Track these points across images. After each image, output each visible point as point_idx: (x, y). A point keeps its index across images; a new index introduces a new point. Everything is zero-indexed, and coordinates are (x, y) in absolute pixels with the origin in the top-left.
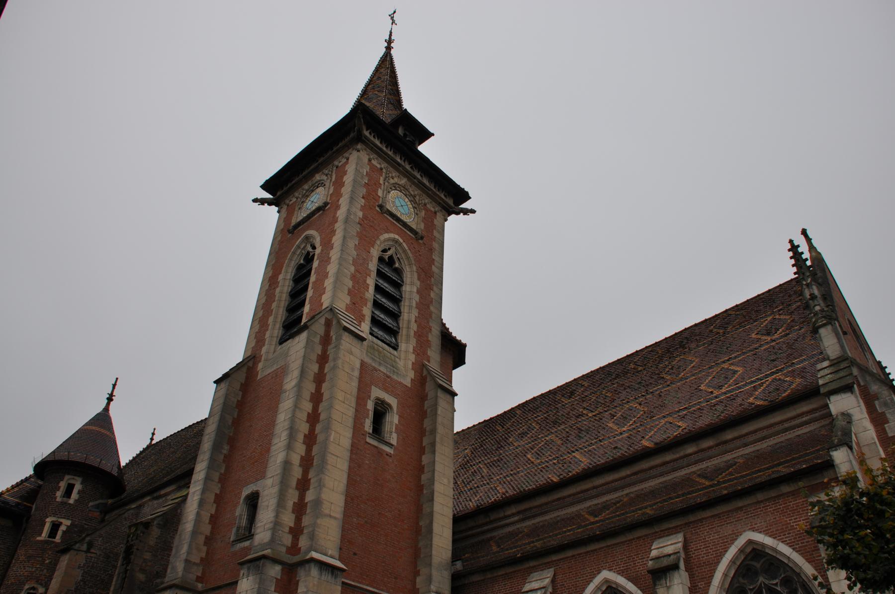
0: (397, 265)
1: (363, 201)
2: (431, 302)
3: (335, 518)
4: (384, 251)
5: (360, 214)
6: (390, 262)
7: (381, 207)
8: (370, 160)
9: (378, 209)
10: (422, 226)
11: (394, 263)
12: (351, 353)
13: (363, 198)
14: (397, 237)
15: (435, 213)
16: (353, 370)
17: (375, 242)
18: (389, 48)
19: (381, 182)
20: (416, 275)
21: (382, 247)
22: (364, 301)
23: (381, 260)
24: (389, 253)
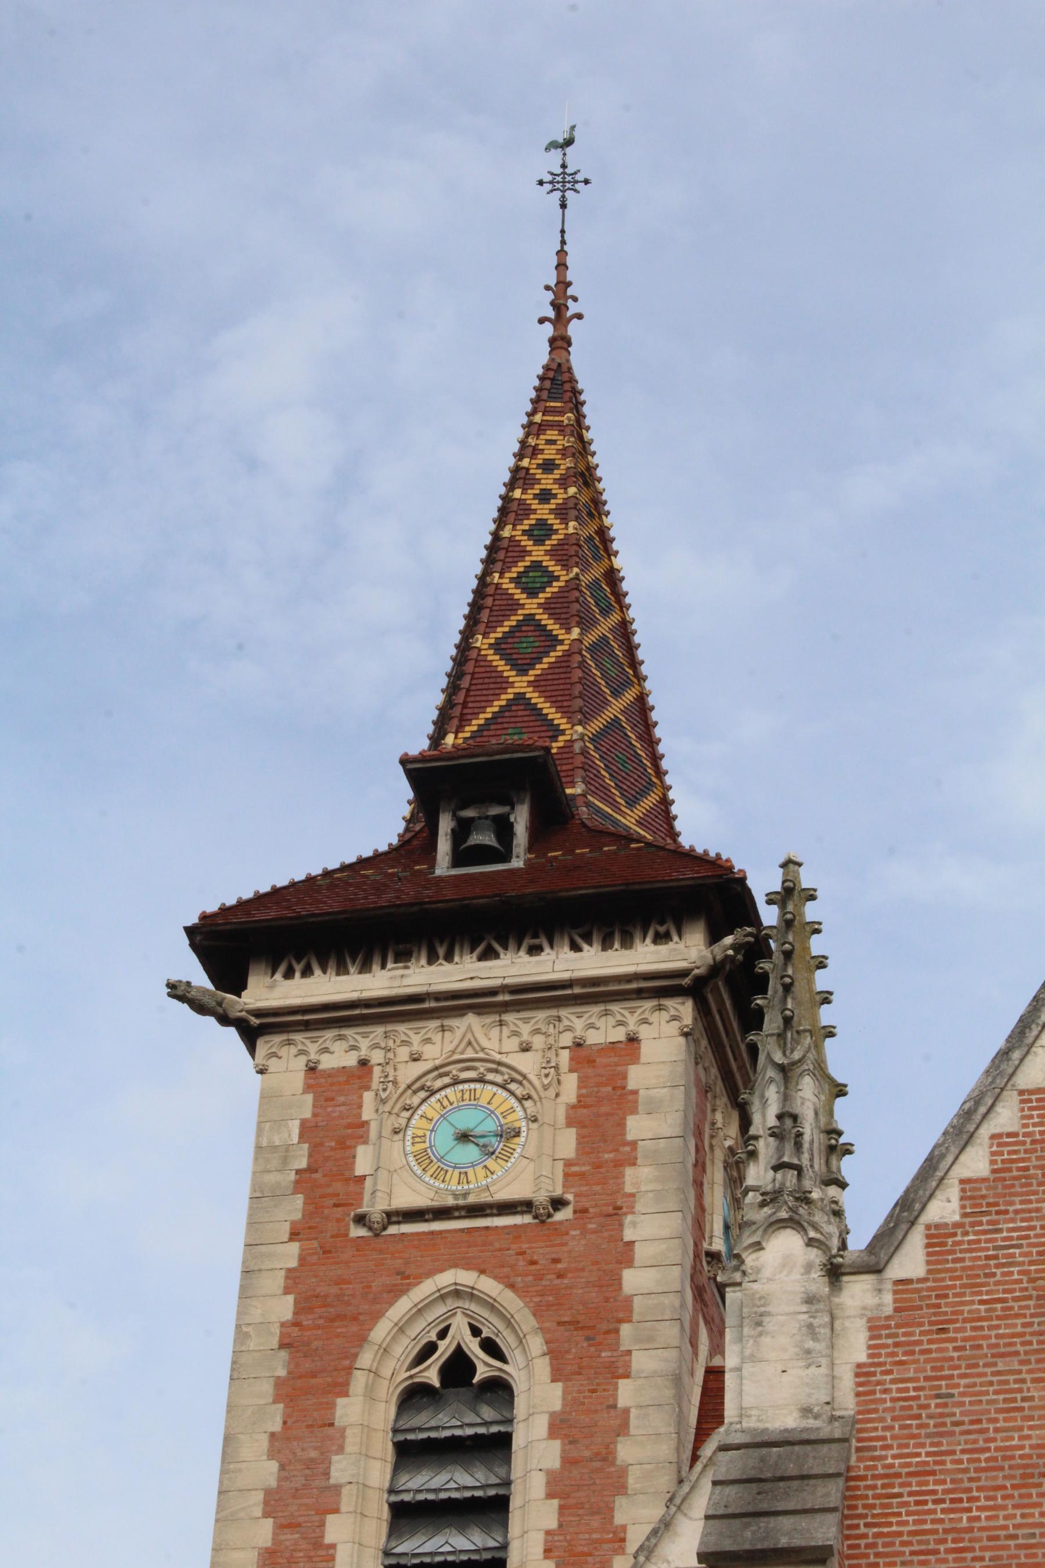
0: (482, 1373)
1: (295, 1247)
2: (623, 1428)
4: (429, 1349)
5: (284, 1308)
6: (458, 1368)
7: (361, 1220)
8: (312, 1069)
9: (358, 1232)
10: (567, 1143)
11: (472, 1369)
14: (446, 1279)
15: (633, 1040)
17: (349, 1370)
18: (560, 343)
19: (367, 1113)
20: (542, 1367)
23: (415, 1396)
24: (445, 1348)
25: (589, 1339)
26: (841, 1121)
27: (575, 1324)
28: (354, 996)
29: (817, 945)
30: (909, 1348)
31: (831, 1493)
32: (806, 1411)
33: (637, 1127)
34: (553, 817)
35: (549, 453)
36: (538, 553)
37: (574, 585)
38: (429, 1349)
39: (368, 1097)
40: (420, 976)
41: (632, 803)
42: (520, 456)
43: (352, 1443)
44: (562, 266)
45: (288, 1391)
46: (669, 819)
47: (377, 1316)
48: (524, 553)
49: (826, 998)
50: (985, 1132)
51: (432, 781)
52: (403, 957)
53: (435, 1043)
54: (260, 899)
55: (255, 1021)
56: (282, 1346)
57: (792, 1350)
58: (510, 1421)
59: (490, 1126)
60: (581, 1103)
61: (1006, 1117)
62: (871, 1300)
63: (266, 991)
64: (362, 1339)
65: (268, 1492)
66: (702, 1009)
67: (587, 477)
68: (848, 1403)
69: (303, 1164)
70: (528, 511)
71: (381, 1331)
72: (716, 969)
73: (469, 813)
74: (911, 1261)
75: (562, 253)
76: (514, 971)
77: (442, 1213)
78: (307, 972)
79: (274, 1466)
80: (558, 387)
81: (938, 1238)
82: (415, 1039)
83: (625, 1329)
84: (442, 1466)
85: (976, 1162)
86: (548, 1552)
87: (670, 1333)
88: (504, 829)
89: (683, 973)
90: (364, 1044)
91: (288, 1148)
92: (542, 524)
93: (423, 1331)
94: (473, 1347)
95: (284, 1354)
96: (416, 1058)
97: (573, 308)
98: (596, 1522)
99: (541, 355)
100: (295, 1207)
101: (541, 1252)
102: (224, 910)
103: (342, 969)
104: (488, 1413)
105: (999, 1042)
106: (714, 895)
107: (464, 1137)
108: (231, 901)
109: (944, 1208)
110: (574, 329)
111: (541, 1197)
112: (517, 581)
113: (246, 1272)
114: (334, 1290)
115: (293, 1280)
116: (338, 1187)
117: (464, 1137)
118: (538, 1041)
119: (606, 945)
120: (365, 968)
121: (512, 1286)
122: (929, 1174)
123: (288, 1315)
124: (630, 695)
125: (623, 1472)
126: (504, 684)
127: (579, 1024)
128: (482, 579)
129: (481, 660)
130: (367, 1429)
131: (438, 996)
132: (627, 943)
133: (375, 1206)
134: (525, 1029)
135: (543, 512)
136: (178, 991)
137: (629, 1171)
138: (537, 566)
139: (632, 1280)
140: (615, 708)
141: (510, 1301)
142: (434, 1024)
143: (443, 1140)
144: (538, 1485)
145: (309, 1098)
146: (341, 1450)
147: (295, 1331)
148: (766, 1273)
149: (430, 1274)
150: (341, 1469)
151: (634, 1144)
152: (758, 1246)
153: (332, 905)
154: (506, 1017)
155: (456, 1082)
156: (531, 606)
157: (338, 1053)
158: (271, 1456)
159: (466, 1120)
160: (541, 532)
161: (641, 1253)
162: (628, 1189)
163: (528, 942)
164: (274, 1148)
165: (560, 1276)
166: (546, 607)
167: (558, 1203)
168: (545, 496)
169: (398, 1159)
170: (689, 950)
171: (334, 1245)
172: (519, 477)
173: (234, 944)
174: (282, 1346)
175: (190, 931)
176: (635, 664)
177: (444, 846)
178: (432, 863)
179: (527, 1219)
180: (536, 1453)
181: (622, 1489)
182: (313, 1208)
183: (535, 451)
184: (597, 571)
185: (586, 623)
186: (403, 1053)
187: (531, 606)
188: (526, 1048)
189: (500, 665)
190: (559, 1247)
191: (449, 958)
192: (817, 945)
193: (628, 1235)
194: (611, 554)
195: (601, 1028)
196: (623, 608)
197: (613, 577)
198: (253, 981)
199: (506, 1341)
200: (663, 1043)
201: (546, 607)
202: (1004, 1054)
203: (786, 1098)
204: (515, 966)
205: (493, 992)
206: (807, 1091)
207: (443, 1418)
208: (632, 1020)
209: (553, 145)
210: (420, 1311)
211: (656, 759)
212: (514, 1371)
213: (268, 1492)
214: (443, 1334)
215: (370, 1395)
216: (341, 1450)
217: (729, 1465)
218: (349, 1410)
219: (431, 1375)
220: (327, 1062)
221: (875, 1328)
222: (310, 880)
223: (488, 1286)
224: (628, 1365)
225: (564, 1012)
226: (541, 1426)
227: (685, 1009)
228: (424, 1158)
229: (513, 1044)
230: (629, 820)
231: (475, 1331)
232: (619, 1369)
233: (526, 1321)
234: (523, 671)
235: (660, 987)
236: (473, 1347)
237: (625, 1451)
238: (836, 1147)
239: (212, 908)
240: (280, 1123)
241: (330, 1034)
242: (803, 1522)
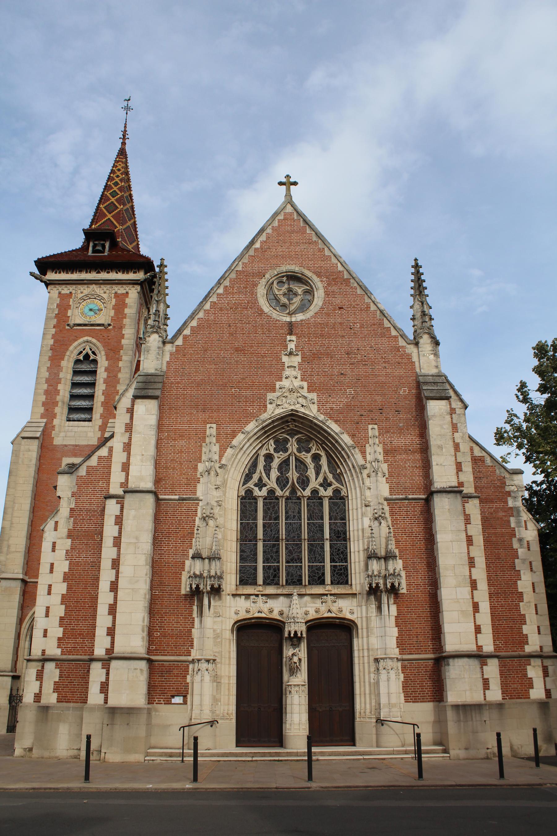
0: (91, 358)
1: (54, 329)
2: (120, 371)
3: (19, 552)
4: (81, 352)
5: (51, 342)
6: (87, 356)
7: (68, 325)
8: (60, 293)
9: (67, 327)
10: (112, 313)
11: (90, 357)
12: (29, 450)
13: (54, 327)
14: (86, 338)
15: (127, 293)
16: (31, 461)
18: (124, 144)
20: (104, 358)
21: (76, 352)
22: (56, 404)
23: (77, 362)
24: (84, 352)
25: (114, 352)
26: (168, 313)
27: (111, 349)
28: (70, 279)
29: (166, 277)
30: (177, 359)
31: (160, 386)
32: (156, 370)
33: (127, 311)
34: (114, 245)
35: (119, 167)
36: (115, 189)
37: (122, 196)
38: (81, 352)
39: (71, 300)
40: (83, 276)
41: (131, 244)
42: (113, 167)
43: (64, 370)
44: (125, 127)
45: (51, 359)
46: (138, 248)
47: (71, 345)
48: (112, 188)
49: (167, 288)
50: (196, 317)
51: (89, 235)
52: (80, 271)
53: (86, 290)
54: (50, 256)
55: (48, 282)
56: (51, 349)
57: (154, 357)
58: (97, 368)
59: (97, 308)
60: (116, 305)
61: (201, 315)
62: (171, 349)
63: (51, 276)
64: (67, 349)
65: (46, 379)
66: (142, 288)
67: (127, 173)
68: (165, 369)
69: (57, 313)
70: (114, 179)
71: (71, 348)
72: (145, 280)
73: (96, 242)
74: (179, 342)
75: (126, 124)
76: (104, 276)
77: (85, 325)
78: (60, 273)
79: (48, 373)
80: (122, 153)
81: (185, 337)
82: (82, 289)
83: (121, 351)
84: (82, 376)
85: (194, 323)
86: (103, 394)
87: (131, 353)
88: (104, 247)
89: (139, 280)
90: (71, 289)
91: (54, 309)
92: (117, 182)
93: (80, 349)
94: (90, 353)
95: (51, 351)
96: (82, 293)
97: (127, 136)
98: (113, 389)
99: (120, 146)
100: (55, 321)
101: (105, 335)
102: (43, 258)
103: (67, 273)
104: (92, 366)
105: (201, 300)
106: (146, 264)
107: (91, 310)
108: (44, 256)
109: (187, 332)
110: (127, 141)
111: (106, 323)
112: (110, 194)
113: (44, 334)
114: (62, 339)
115: (53, 336)
116: (64, 318)
117: (91, 310)
118: (108, 291)
119: (123, 273)
120: (72, 273)
121: (99, 341)
122: (185, 325)
123: (52, 343)
124: (132, 221)
125: (119, 379)
126: (106, 216)
127: (116, 289)
128: (103, 193)
129: (101, 210)
130: (67, 367)
131: (87, 280)
132: (128, 273)
133: (72, 323)
134: (105, 289)
135: (117, 180)
136: (32, 274)
137: (124, 320)
138: (115, 191)
139: (123, 342)
140: (129, 223)
141: (98, 344)
142: (86, 286)
143: (87, 310)
144: (102, 381)
145: (59, 299)
146: (62, 371)
147: (53, 347)
148: (151, 342)
149: (82, 337)
150: (61, 375)
151: (126, 314)
152: (149, 336)
153: (66, 259)
154: (101, 286)
155: (90, 298)
156: (113, 200)
157: (65, 290)
158: (47, 371)
159: (91, 306)
160: (116, 184)
161: (126, 336)
162: (124, 323)
163: (107, 271)
164: (51, 309)
165: (109, 340)
166: (116, 200)
167: (109, 325)
168: (118, 176)
169: (77, 313)
170: (140, 276)
171: (62, 331)
172: (112, 172)
173: (45, 265)
174: (51, 349)
175: (35, 262)
176: (134, 215)
177: (91, 249)
178: (88, 252)
179: (103, 328)
180: (102, 374)
181: (119, 383)
182: (58, 322)
183: (116, 166)
184: (127, 194)
185: (124, 205)
186: (79, 291)
187: (113, 200)
188: (105, 293)
189: (105, 212)
190: (109, 334)
191: (90, 272)
192: (166, 277)
193: (123, 332)
194: (131, 190)
195: (121, 290)
196: (132, 202)
197: (131, 196)
198: (48, 273)
199: (97, 352)
200: (134, 293)
201: (116, 200)
202: (202, 302)
203: (157, 307)
204: (104, 275)
205: (99, 280)
206: (162, 306)
207: (83, 366)
208: (127, 289)
209: (126, 100)
210: (79, 345)
211: (137, 235)
212: (98, 358)
213: (46, 379)
214: (84, 350)
215: (68, 360)
216: (62, 371)
217: (140, 379)
218: (64, 363)
219: (81, 358)
220: (63, 292)
221: (171, 354)
222: (62, 253)
223: (94, 340)
224: (121, 358)
225: (113, 286)
226: (103, 369)
227: (139, 288)
228: (82, 313)
229: (102, 292)
230: (130, 247)
231: (91, 349)
232: (120, 359)
233: (101, 348)
234: (110, 213)
235: (134, 283)
236: (90, 353)
237: (120, 375)
238: (166, 318)
239: (40, 257)
240: (52, 304)
241: (64, 286)
242: (154, 391)
